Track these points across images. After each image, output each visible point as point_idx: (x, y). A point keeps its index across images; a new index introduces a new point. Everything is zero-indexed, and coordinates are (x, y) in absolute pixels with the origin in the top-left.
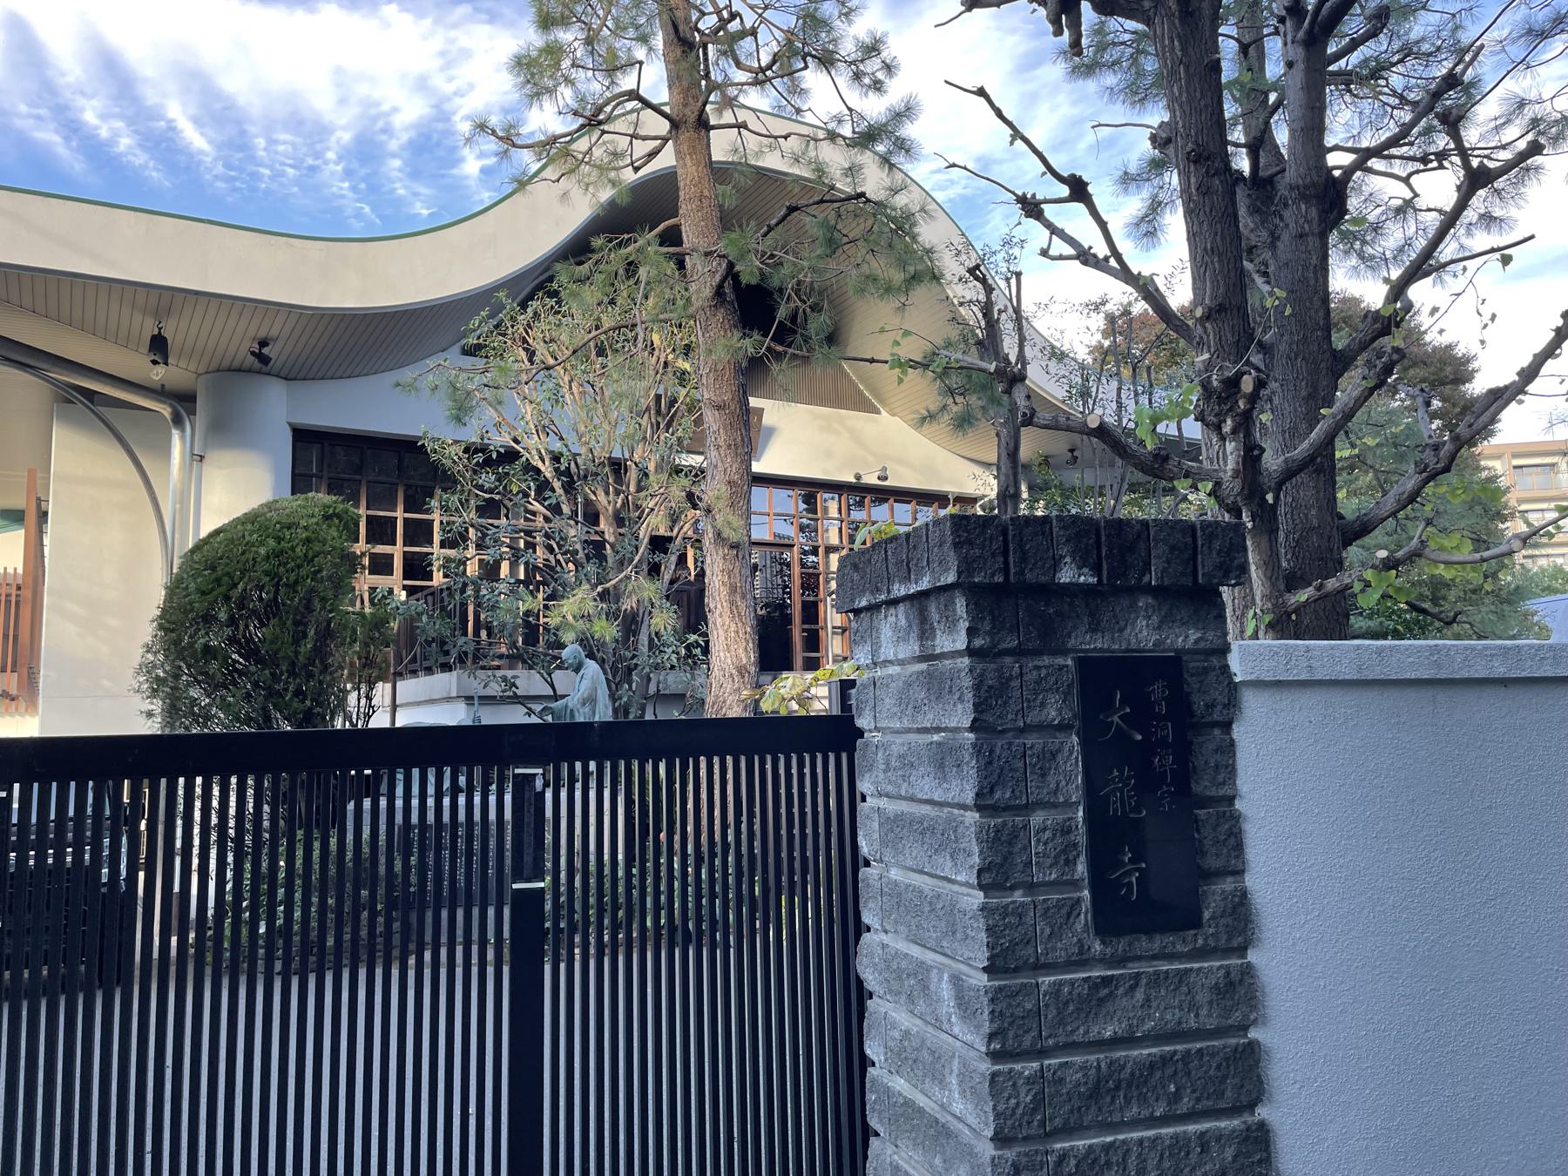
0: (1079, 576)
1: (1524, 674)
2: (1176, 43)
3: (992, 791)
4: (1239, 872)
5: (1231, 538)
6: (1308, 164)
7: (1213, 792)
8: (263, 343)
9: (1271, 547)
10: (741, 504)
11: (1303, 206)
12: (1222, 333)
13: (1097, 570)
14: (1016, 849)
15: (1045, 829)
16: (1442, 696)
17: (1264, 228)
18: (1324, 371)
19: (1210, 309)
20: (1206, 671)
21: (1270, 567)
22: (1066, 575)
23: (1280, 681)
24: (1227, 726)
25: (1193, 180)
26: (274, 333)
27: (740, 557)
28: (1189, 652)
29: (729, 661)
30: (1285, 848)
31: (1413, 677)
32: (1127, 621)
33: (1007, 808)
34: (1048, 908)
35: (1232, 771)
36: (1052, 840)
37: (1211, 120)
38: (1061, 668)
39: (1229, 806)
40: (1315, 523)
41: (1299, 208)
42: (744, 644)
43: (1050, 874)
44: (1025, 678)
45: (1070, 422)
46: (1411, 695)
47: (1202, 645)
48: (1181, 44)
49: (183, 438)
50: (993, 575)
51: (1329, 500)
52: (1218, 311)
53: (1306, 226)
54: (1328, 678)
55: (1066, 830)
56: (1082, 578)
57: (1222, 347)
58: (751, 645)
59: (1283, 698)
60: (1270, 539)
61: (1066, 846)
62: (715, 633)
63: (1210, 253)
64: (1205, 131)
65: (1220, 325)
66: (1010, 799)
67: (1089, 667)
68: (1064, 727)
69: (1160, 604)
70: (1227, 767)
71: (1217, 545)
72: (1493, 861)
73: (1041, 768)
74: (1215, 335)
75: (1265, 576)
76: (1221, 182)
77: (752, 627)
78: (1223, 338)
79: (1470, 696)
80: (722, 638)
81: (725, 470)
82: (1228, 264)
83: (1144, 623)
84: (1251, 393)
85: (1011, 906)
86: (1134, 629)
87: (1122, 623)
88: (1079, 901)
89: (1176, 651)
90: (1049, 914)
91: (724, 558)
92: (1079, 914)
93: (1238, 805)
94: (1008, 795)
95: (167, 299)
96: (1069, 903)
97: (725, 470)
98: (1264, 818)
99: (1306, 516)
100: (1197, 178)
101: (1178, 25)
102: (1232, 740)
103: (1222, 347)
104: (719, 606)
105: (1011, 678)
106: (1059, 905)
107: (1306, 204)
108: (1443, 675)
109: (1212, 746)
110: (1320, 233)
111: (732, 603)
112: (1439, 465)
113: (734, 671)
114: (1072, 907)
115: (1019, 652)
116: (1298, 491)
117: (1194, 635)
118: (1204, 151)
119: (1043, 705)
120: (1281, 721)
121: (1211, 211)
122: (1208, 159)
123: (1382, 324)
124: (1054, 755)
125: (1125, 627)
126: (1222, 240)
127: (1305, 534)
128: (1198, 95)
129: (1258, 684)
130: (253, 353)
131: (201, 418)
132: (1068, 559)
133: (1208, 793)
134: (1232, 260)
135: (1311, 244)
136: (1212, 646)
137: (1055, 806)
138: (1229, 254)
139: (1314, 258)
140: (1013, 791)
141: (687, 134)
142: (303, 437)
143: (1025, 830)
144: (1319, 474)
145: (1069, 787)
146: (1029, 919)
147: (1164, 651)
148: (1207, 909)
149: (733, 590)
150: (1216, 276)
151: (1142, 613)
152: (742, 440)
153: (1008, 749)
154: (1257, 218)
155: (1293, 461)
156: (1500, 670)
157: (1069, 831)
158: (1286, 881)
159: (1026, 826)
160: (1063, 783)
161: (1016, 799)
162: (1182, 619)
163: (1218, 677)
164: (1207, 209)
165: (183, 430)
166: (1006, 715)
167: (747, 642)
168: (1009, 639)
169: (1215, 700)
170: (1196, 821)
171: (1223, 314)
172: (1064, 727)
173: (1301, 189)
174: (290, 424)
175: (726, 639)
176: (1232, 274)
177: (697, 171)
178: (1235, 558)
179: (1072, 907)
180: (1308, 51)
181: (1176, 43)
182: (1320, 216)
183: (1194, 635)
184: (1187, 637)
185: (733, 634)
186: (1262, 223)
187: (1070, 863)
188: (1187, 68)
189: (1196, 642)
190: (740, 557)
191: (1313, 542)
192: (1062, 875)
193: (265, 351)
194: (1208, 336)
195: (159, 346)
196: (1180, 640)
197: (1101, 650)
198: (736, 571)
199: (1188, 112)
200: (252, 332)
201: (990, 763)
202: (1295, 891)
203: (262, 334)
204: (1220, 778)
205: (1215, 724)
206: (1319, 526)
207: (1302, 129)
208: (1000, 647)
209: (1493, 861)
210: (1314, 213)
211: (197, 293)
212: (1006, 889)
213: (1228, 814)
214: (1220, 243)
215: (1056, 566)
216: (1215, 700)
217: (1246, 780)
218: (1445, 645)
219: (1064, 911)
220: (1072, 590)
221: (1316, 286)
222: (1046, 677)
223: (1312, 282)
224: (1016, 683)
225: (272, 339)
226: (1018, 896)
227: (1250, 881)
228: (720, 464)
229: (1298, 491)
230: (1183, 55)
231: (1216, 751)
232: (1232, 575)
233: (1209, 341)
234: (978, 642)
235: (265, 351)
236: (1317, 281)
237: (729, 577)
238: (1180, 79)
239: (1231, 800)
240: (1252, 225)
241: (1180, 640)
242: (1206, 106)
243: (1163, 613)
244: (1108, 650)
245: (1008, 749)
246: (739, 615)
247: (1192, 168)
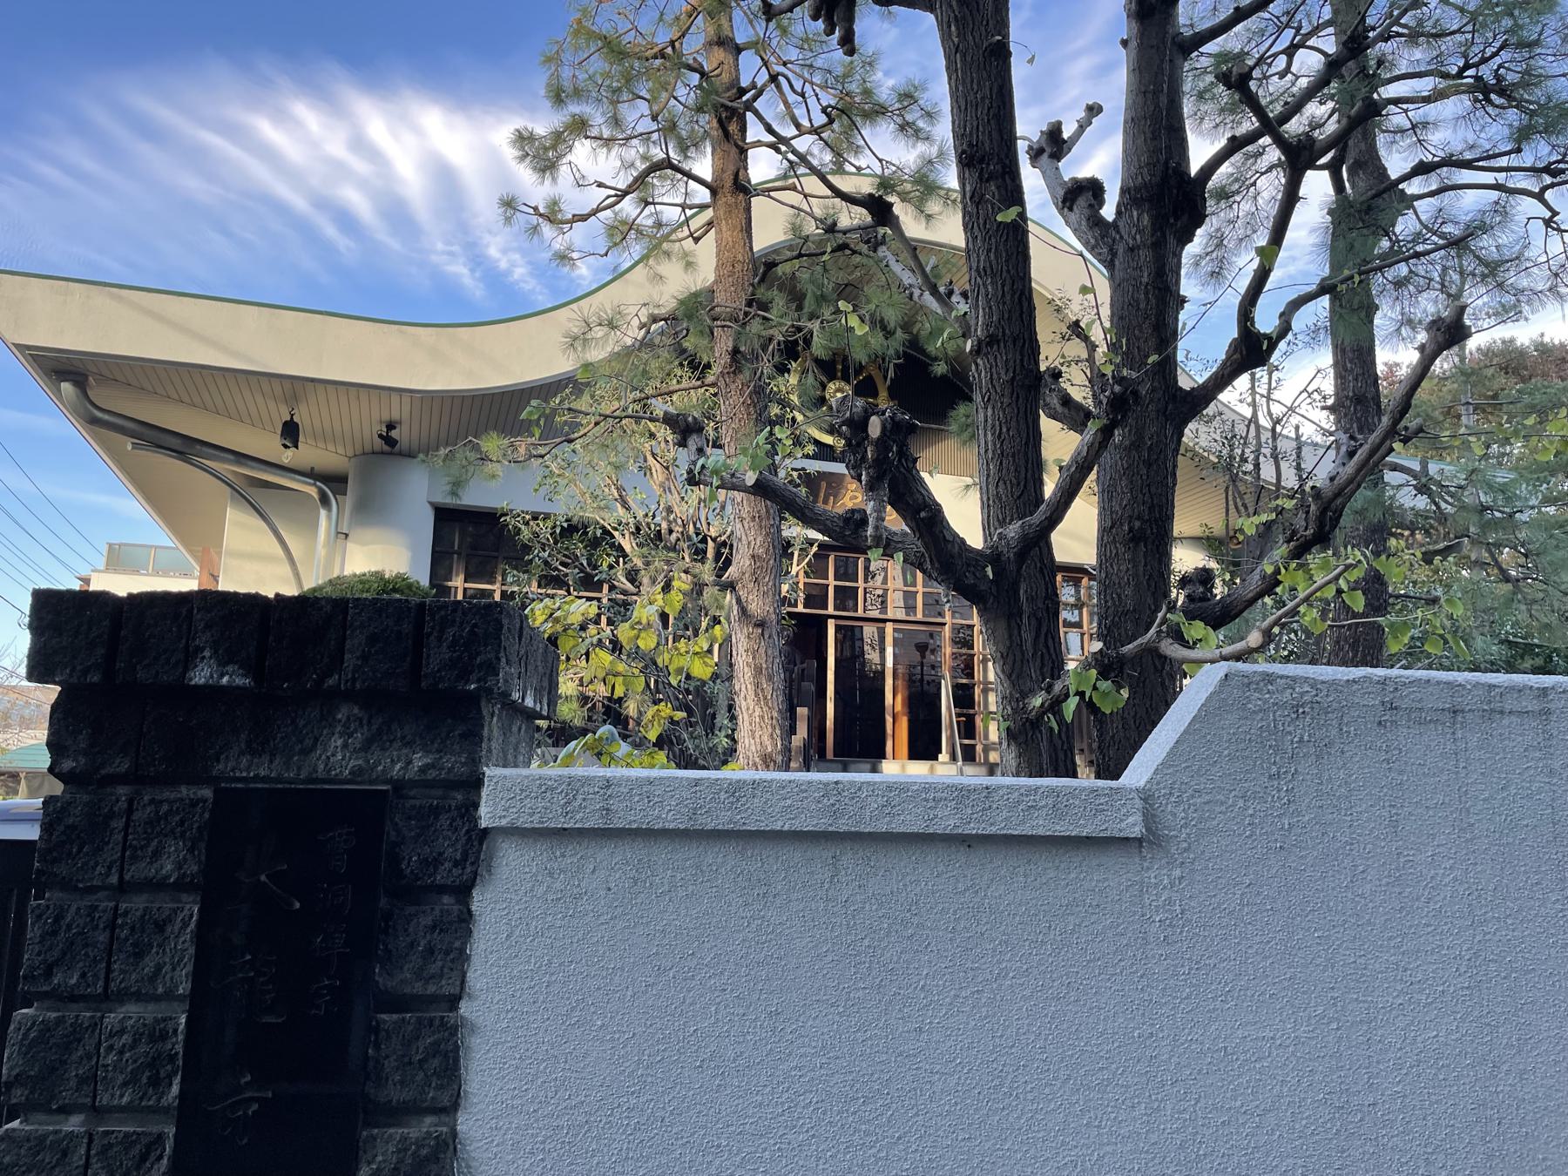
0: (222, 676)
1: (993, 830)
2: (953, 28)
3: (48, 974)
4: (453, 1107)
5: (475, 625)
6: (1139, 160)
7: (418, 988)
8: (391, 426)
9: (1010, 636)
10: (767, 579)
11: (1135, 213)
12: (994, 370)
13: (250, 668)
14: (75, 1057)
15: (122, 1031)
16: (849, 859)
17: (1104, 244)
18: (1153, 415)
19: (980, 342)
20: (436, 812)
21: (1011, 657)
22: (201, 676)
23: (565, 829)
24: (464, 892)
25: (968, 188)
26: (395, 416)
27: (766, 636)
28: (413, 783)
29: (753, 748)
30: (536, 1076)
31: (786, 828)
32: (316, 739)
33: (73, 999)
34: (111, 1146)
35: (460, 959)
36: (132, 1048)
37: (988, 115)
38: (194, 803)
39: (451, 1011)
40: (1130, 605)
41: (1131, 216)
42: (770, 730)
43: (122, 1096)
44: (135, 816)
45: (734, 480)
46: (794, 855)
47: (432, 774)
48: (958, 29)
49: (329, 518)
50: (85, 672)
51: (1151, 575)
52: (989, 344)
53: (1138, 237)
54: (634, 826)
55: (158, 1033)
56: (225, 680)
57: (994, 387)
58: (778, 732)
59: (568, 853)
60: (1009, 626)
61: (154, 1059)
62: (740, 717)
63: (983, 274)
64: (981, 128)
65: (992, 361)
66: (78, 985)
67: (231, 802)
68: (181, 886)
69: (370, 717)
70: (447, 953)
71: (450, 633)
72: (917, 1115)
73: (135, 945)
74: (986, 372)
75: (1003, 671)
76: (998, 188)
77: (780, 711)
78: (995, 376)
79: (903, 862)
80: (746, 723)
81: (749, 543)
82: (1003, 286)
83: (339, 742)
84: (878, 439)
85: (51, 1138)
86: (325, 750)
87: (308, 742)
88: (160, 1138)
89: (390, 781)
90: (111, 1153)
91: (749, 637)
92: (160, 1157)
93: (465, 1008)
94: (73, 981)
95: (295, 387)
96: (144, 1140)
97: (749, 543)
98: (504, 1030)
99: (1119, 596)
100: (971, 186)
101: (955, 7)
102: (470, 912)
103: (994, 387)
104: (743, 689)
105: (111, 815)
106: (128, 1141)
107: (1138, 210)
108: (843, 826)
109: (427, 920)
110: (1153, 244)
111: (757, 685)
112: (1308, 532)
113: (757, 760)
114: (149, 1148)
115: (135, 778)
116: (1112, 566)
117: (419, 760)
118: (977, 151)
119: (157, 854)
120: (558, 885)
121: (985, 223)
122: (981, 161)
123: (1241, 353)
124: (160, 927)
125: (313, 748)
126: (996, 257)
127: (1117, 619)
128: (975, 87)
129: (514, 832)
130: (380, 436)
131: (349, 500)
132: (207, 653)
133: (407, 990)
134: (1008, 282)
135: (1142, 258)
136: (451, 776)
137: (157, 999)
138: (1004, 274)
139: (1146, 274)
140: (83, 975)
141: (724, 200)
142: (446, 517)
143: (93, 1032)
144: (1137, 544)
145: (177, 973)
146: (78, 1158)
147: (371, 782)
148: (369, 1163)
149: (758, 671)
150: (988, 302)
151: (339, 729)
152: (767, 511)
153: (89, 915)
154: (1097, 232)
155: (1030, 526)
156: (1039, 826)
157: (164, 1036)
158: (528, 1127)
159: (95, 1025)
160: (168, 968)
161: (89, 986)
162: (403, 738)
163: (453, 820)
164: (981, 221)
165: (330, 510)
166: (94, 869)
167: (774, 728)
168: (118, 761)
169: (441, 854)
170: (377, 1030)
171: (995, 347)
172: (181, 886)
173: (1133, 192)
174: (430, 503)
175: (751, 724)
176: (1008, 297)
177: (732, 236)
178: (478, 654)
179: (149, 1148)
180: (1142, 23)
181: (953, 28)
182: (1153, 224)
183: (419, 760)
184: (409, 762)
185: (757, 720)
186: (1102, 238)
187: (158, 1083)
188: (964, 56)
189: (423, 770)
190: (766, 636)
191: (1126, 630)
192: (141, 1099)
193: (394, 434)
194: (980, 375)
195: (291, 432)
196: (398, 767)
197: (265, 779)
198: (762, 651)
199: (963, 108)
200: (376, 416)
201: (54, 933)
202: (543, 1142)
203: (386, 417)
204: (434, 968)
205: (442, 889)
206: (1134, 610)
207: (1132, 119)
208: (103, 772)
209: (917, 1115)
210: (1146, 219)
211: (313, 380)
212: (50, 1112)
213: (437, 1022)
214: (994, 262)
215: (189, 659)
216: (441, 854)
217: (478, 975)
218: (852, 783)
219: (136, 1151)
220: (211, 693)
221: (1146, 309)
222: (166, 814)
223: (1142, 306)
224: (118, 824)
225: (397, 423)
226: (74, 1124)
227: (465, 1123)
228: (744, 537)
229: (1112, 566)
230: (959, 42)
231: (434, 927)
232: (474, 677)
233: (980, 381)
234: (68, 765)
235: (394, 434)
236: (1147, 304)
237: (754, 658)
238: (956, 70)
239: (454, 1001)
240: (1093, 241)
241: (398, 767)
242: (983, 98)
243: (374, 727)
244: (279, 780)
245: (89, 915)
246: (765, 698)
247: (967, 175)
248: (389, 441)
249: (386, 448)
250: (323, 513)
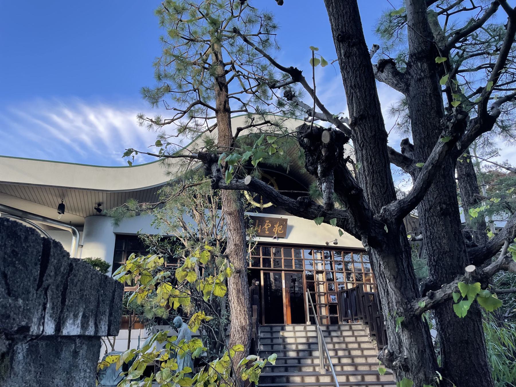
6: (419, 41)
8: (99, 205)
9: (398, 265)
10: (241, 254)
11: (419, 64)
12: (364, 131)
17: (402, 82)
21: (399, 279)
25: (342, 51)
26: (101, 201)
27: (241, 277)
29: (237, 324)
37: (349, 18)
40: (447, 248)
41: (417, 66)
42: (244, 316)
45: (238, 183)
49: (76, 240)
51: (455, 232)
53: (422, 74)
57: (365, 139)
58: (247, 316)
60: (396, 259)
62: (232, 311)
64: (347, 25)
74: (360, 133)
75: (396, 287)
76: (358, 49)
77: (248, 308)
78: (365, 134)
80: (234, 313)
81: (233, 240)
82: (365, 92)
84: (329, 143)
91: (234, 278)
95: (63, 191)
97: (233, 240)
99: (440, 244)
103: (365, 139)
104: (233, 299)
111: (238, 297)
113: (239, 329)
116: (433, 229)
121: (353, 65)
123: (480, 124)
126: (360, 80)
128: (342, 8)
130: (95, 208)
131: (84, 233)
138: (365, 87)
139: (429, 90)
141: (221, 114)
142: (120, 238)
149: (238, 291)
152: (240, 227)
164: (350, 64)
165: (76, 237)
167: (245, 315)
174: (114, 233)
175: (236, 314)
176: (368, 97)
177: (224, 127)
185: (239, 312)
190: (241, 277)
191: (447, 261)
193: (101, 207)
194: (357, 134)
195: (61, 208)
198: (240, 283)
200: (94, 201)
203: (97, 201)
206: (450, 251)
210: (425, 65)
211: (70, 188)
221: (431, 105)
223: (429, 103)
225: (101, 203)
228: (231, 237)
229: (433, 229)
233: (357, 137)
235: (101, 207)
236: (432, 103)
237: (237, 286)
238: (332, 3)
240: (395, 82)
246: (242, 303)
247: (341, 46)
248: (99, 210)
249: (98, 213)
250: (74, 238)
